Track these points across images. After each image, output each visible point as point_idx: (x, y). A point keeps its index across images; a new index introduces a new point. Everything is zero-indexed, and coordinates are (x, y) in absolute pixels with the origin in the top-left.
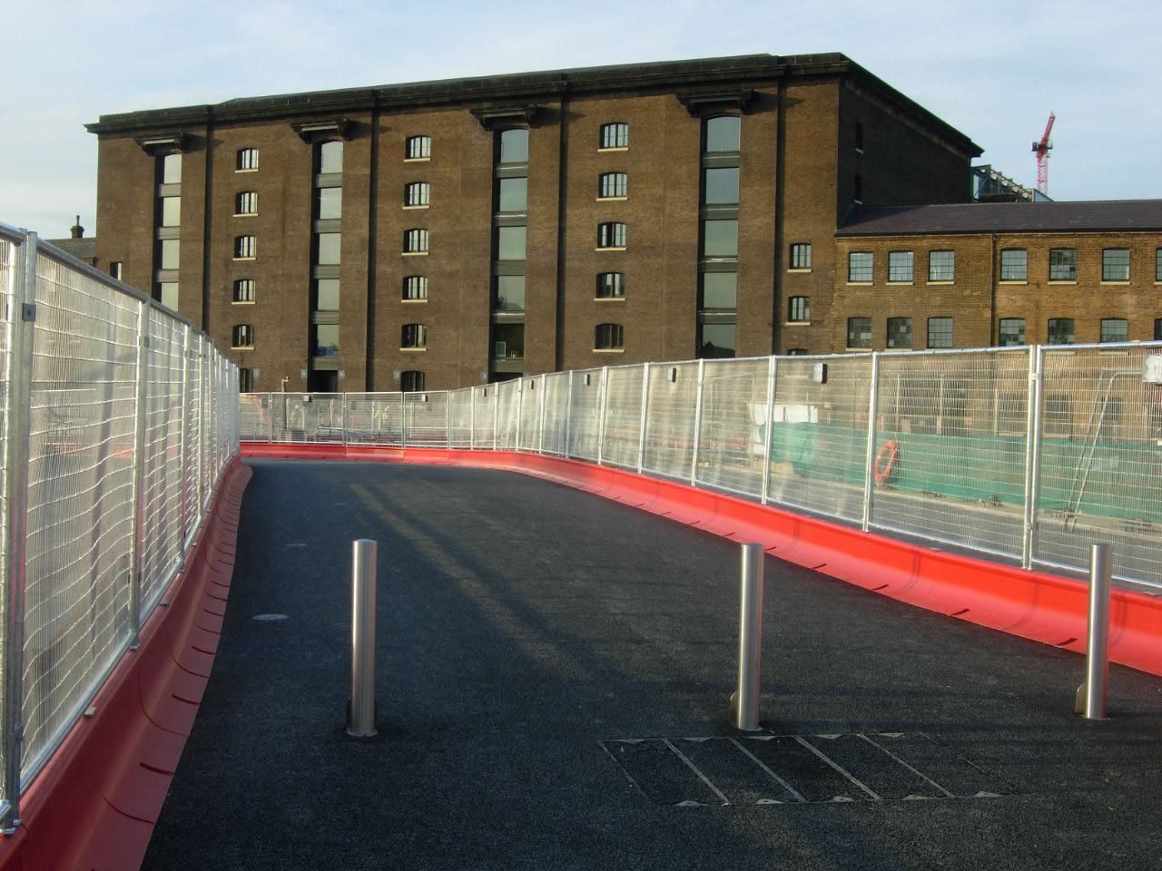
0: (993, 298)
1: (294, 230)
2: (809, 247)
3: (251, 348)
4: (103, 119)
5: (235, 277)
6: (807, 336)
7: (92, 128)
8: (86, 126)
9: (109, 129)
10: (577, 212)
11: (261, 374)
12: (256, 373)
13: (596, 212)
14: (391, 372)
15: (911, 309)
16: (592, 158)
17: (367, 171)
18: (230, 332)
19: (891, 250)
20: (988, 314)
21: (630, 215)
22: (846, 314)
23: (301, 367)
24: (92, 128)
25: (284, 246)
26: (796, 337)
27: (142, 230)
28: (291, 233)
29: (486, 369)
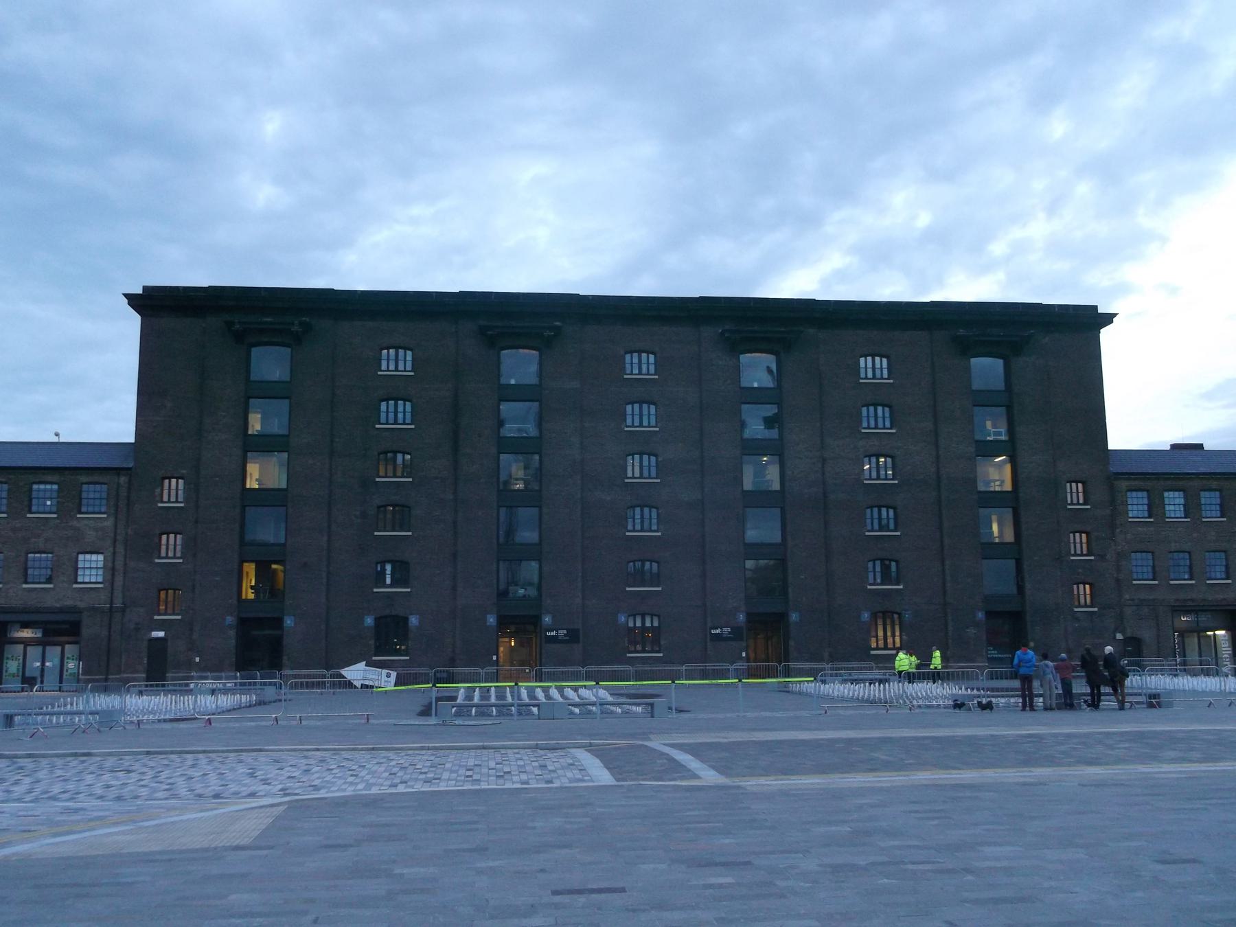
8: (126, 295)
9: (153, 304)
12: (414, 620)
13: (861, 443)
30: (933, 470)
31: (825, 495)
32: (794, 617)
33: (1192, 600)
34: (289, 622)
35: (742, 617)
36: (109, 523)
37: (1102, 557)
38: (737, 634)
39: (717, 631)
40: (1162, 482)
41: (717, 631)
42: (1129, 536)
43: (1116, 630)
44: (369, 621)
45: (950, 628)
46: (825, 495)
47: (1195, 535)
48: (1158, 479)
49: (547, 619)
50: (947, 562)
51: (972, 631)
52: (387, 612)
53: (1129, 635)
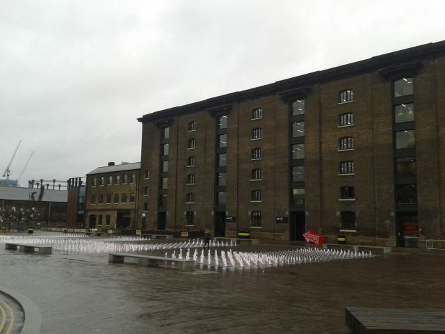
4: (144, 116)
5: (188, 174)
7: (140, 120)
9: (145, 120)
11: (197, 213)
12: (195, 213)
13: (338, 133)
24: (140, 120)
31: (321, 158)
32: (307, 213)
34: (167, 213)
35: (287, 213)
38: (285, 220)
39: (278, 219)
41: (278, 219)
44: (185, 213)
45: (377, 220)
46: (321, 158)
49: (227, 213)
50: (376, 187)
51: (388, 222)
52: (189, 210)
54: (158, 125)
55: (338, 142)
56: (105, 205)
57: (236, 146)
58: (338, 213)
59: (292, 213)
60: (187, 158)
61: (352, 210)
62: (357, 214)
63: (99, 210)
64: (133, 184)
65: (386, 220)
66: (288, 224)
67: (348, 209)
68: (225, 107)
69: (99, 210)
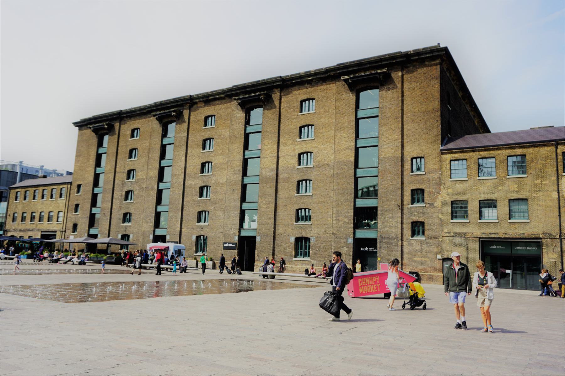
0: (558, 185)
1: (152, 165)
2: (423, 160)
3: (130, 224)
5: (126, 189)
6: (423, 213)
9: (82, 125)
10: (287, 148)
12: (131, 237)
13: (297, 147)
14: (192, 236)
15: (496, 194)
16: (295, 118)
17: (186, 134)
18: (122, 217)
19: (479, 157)
20: (555, 195)
21: (316, 147)
22: (449, 199)
23: (150, 234)
25: (147, 174)
26: (416, 214)
27: (91, 169)
28: (150, 167)
29: (237, 234)
30: (332, 157)
32: (258, 239)
33: (496, 234)
35: (236, 239)
36: (65, 201)
37: (432, 205)
40: (477, 153)
42: (449, 191)
43: (438, 252)
45: (333, 247)
47: (500, 188)
48: (473, 151)
52: (124, 233)
53: (446, 256)
54: (96, 131)
55: (297, 157)
56: (28, 224)
57: (183, 158)
58: (292, 240)
59: (241, 238)
60: (126, 171)
61: (308, 236)
62: (313, 241)
63: (20, 231)
64: (63, 201)
65: (343, 247)
66: (236, 251)
67: (304, 234)
68: (174, 111)
69: (20, 231)
